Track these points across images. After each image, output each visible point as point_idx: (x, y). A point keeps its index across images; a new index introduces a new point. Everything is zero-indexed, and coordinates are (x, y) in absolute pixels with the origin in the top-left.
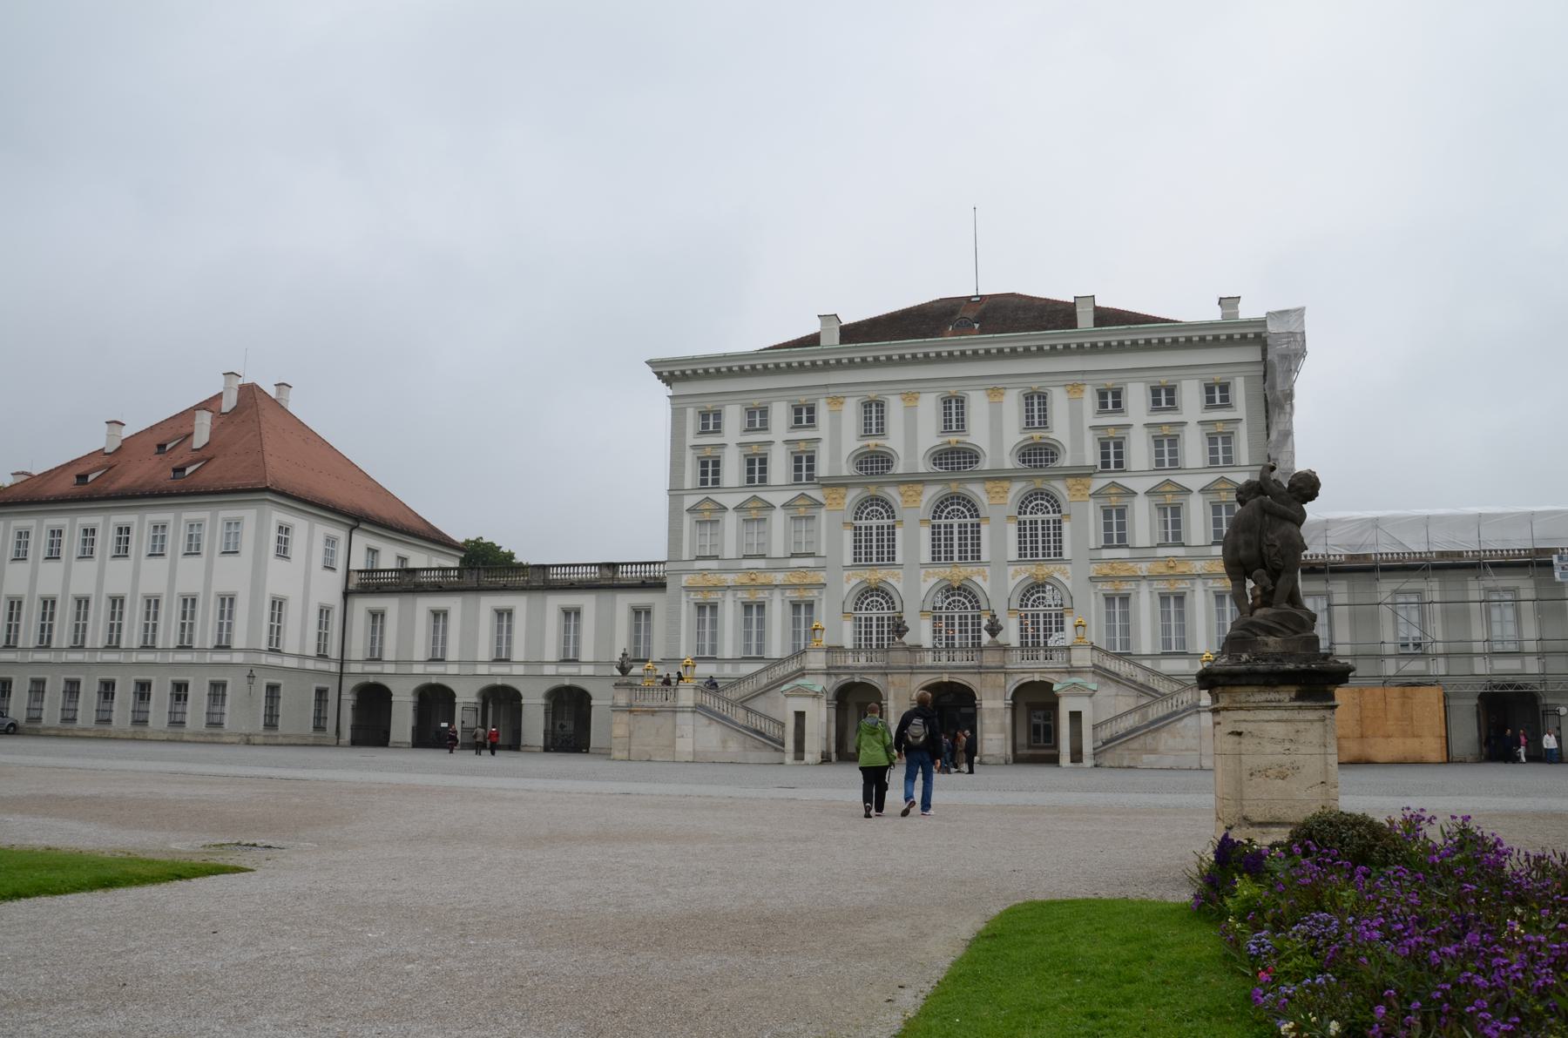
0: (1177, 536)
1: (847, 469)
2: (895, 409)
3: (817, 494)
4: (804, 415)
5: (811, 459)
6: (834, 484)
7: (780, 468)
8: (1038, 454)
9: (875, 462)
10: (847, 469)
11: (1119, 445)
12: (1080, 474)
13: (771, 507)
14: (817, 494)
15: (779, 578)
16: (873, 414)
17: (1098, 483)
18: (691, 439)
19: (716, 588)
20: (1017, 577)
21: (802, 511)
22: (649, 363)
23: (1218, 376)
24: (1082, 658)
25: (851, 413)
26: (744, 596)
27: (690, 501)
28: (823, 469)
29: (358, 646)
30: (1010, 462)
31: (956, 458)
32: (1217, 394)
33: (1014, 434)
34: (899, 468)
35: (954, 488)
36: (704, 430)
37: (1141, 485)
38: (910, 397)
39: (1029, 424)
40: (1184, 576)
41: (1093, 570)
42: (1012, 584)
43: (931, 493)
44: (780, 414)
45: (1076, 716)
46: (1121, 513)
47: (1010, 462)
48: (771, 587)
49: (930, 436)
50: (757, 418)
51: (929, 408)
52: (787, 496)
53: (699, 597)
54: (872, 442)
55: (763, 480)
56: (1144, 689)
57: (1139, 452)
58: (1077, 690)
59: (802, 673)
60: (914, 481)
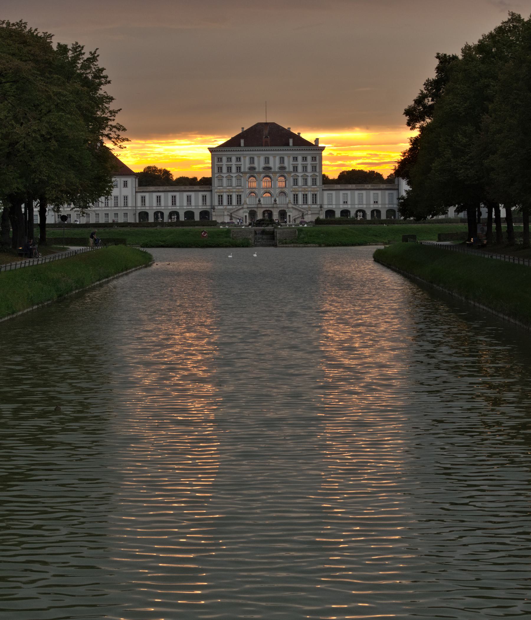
0: (306, 184)
1: (247, 170)
2: (256, 159)
3: (241, 175)
4: (238, 159)
5: (240, 168)
6: (245, 173)
7: (234, 169)
8: (282, 168)
9: (252, 169)
10: (247, 170)
11: (296, 167)
12: (290, 173)
13: (232, 177)
14: (241, 175)
15: (234, 190)
16: (252, 160)
17: (292, 174)
18: (216, 163)
19: (222, 192)
20: (278, 191)
21: (239, 179)
22: (209, 148)
23: (314, 156)
24: (290, 206)
25: (247, 159)
26: (228, 194)
27: (216, 175)
28: (242, 170)
29: (139, 203)
30: (277, 170)
31: (268, 169)
32: (314, 159)
33: (278, 165)
34: (257, 170)
35: (267, 174)
36: (218, 161)
37: (300, 175)
38: (259, 157)
39: (280, 163)
40: (307, 191)
41: (291, 190)
42: (277, 192)
43: (263, 175)
44: (234, 159)
45: (289, 216)
46: (297, 179)
47: (277, 170)
48: (233, 192)
49: (262, 165)
50: (229, 159)
51: (262, 159)
52: (236, 175)
53: (219, 194)
54: (252, 165)
55: (230, 171)
56: (300, 211)
57: (300, 169)
58: (290, 212)
59: (243, 208)
60: (260, 173)
